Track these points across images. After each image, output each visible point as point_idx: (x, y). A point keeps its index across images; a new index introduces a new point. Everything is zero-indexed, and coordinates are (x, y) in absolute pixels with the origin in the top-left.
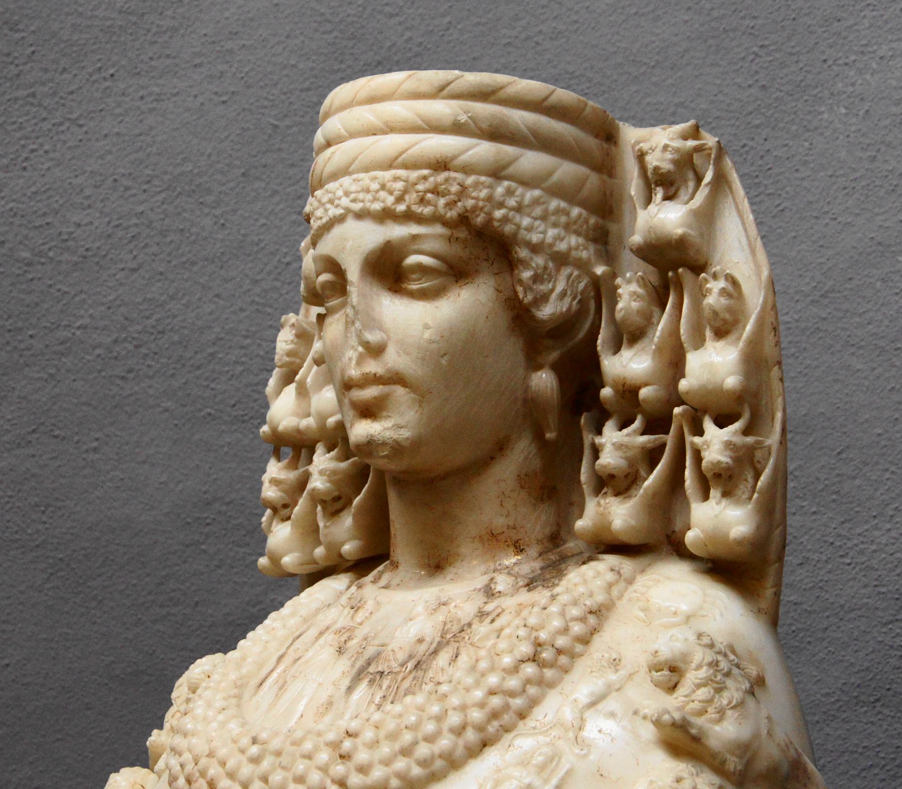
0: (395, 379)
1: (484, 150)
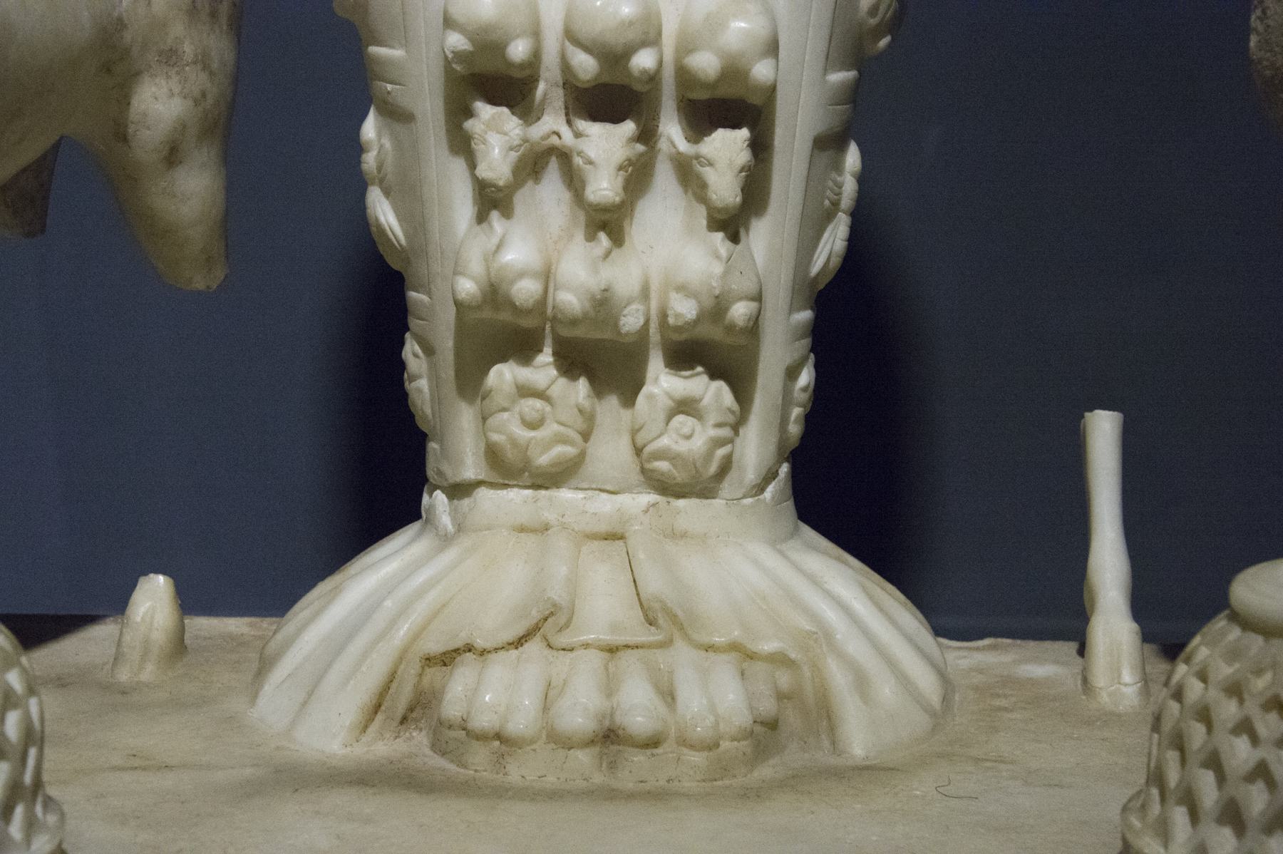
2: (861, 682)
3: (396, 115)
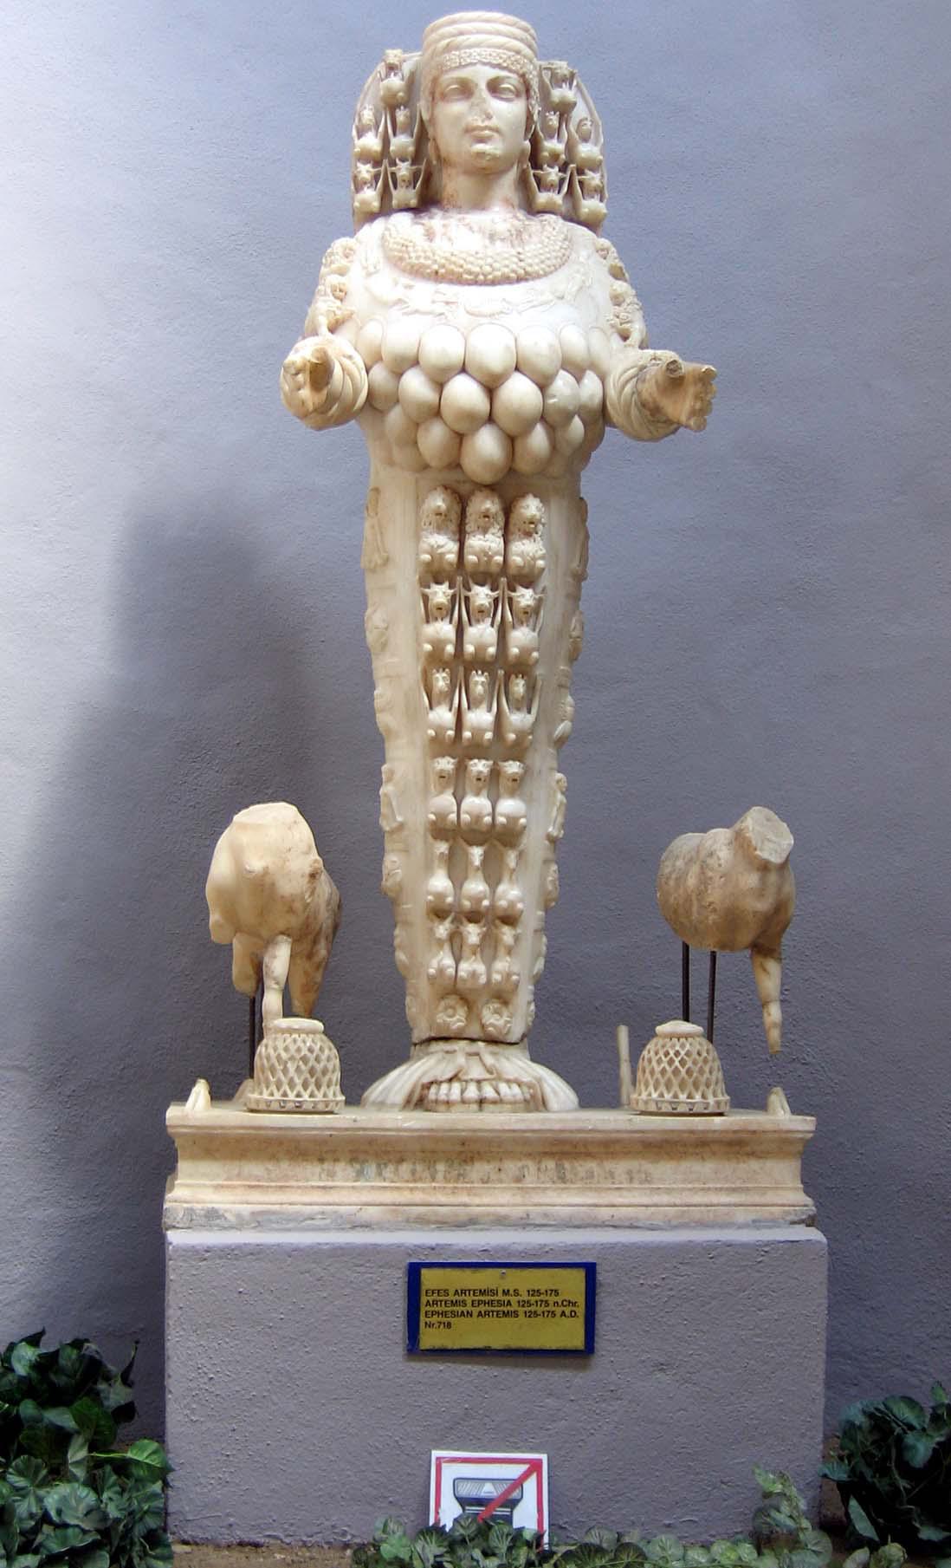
0: (497, 130)
1: (527, 51)
2: (555, 1093)
3: (407, 924)
